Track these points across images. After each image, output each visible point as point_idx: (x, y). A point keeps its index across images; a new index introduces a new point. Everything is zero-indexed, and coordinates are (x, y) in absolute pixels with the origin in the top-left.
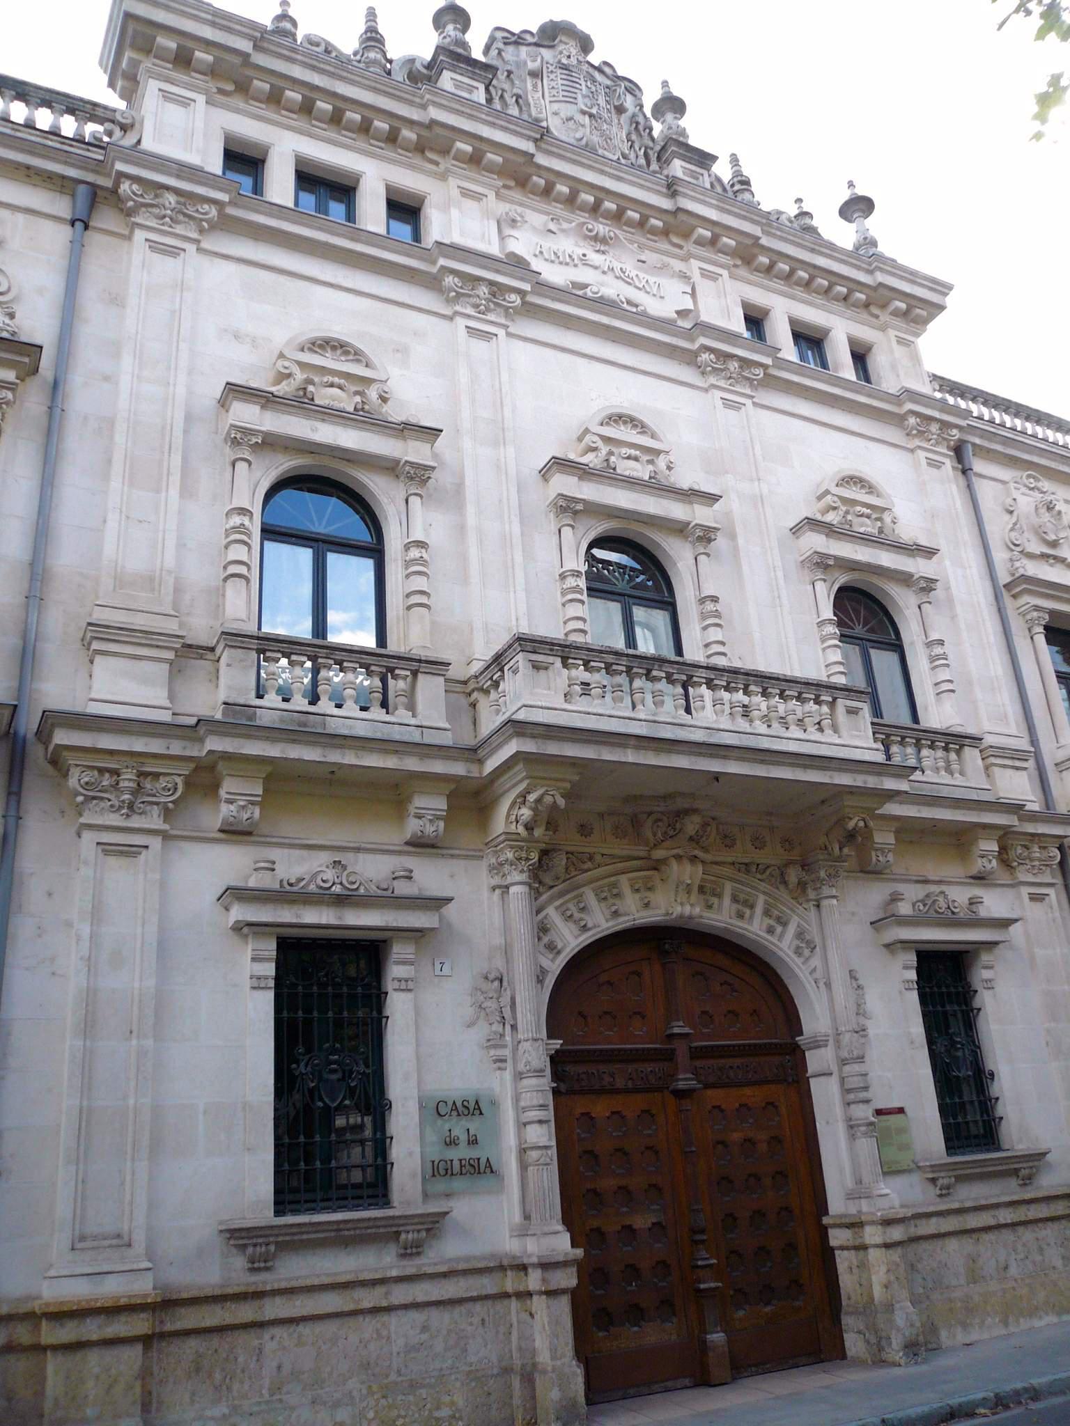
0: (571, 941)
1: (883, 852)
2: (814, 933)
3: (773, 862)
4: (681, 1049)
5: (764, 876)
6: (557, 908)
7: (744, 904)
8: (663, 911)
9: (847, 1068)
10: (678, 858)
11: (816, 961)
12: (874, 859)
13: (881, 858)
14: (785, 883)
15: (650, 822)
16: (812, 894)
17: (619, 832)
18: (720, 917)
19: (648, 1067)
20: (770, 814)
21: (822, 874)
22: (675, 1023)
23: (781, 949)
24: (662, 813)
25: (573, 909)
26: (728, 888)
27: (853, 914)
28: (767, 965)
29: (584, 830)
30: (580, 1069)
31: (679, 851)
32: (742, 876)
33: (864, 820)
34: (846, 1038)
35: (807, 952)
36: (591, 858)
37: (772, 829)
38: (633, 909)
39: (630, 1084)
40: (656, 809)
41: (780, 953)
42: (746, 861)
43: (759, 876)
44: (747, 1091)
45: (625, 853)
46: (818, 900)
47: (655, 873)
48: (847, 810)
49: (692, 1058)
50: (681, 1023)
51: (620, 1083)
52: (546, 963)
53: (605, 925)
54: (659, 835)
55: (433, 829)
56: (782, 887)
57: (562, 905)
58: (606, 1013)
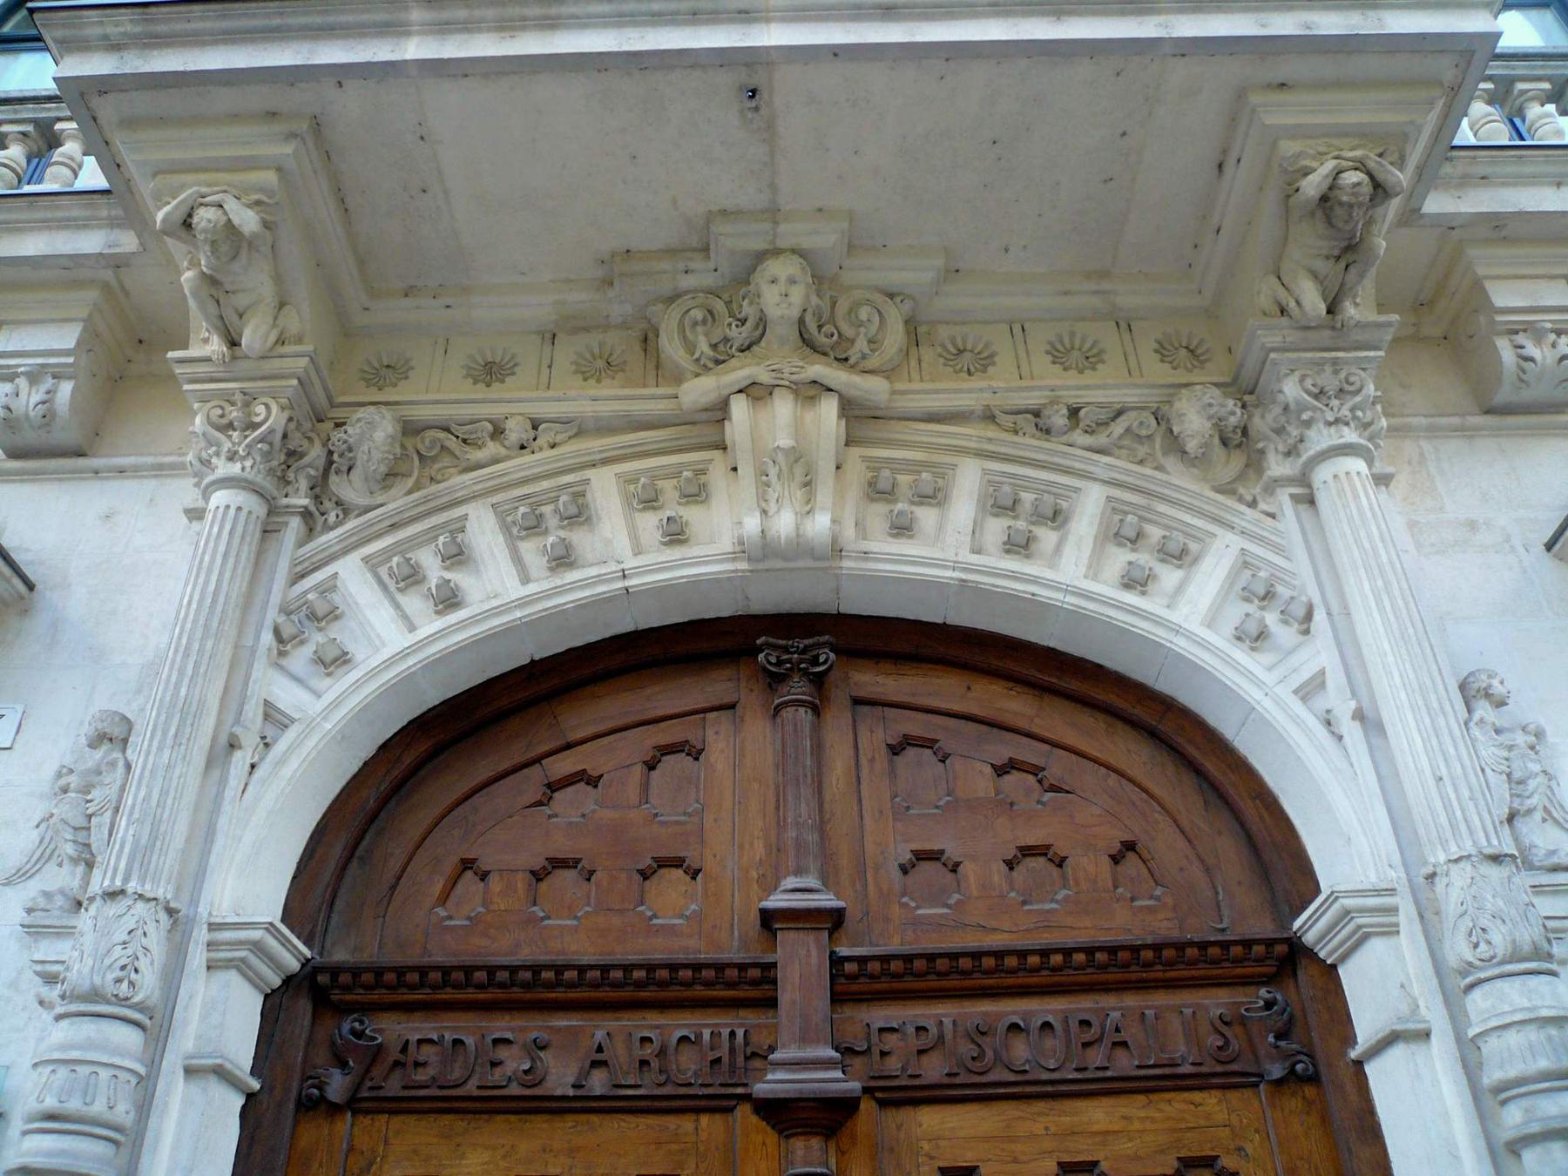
0: (395, 639)
1: (1538, 341)
2: (1302, 576)
3: (1129, 396)
4: (801, 964)
5: (1101, 439)
6: (371, 563)
7: (1028, 518)
8: (726, 544)
9: (1478, 1002)
10: (755, 391)
11: (1319, 654)
12: (1508, 355)
13: (1532, 350)
14: (1175, 445)
15: (675, 313)
16: (1277, 467)
17: (602, 367)
18: (943, 555)
19: (679, 1024)
20: (1104, 274)
21: (1291, 390)
22: (791, 882)
23: (1177, 630)
24: (710, 292)
25: (429, 561)
26: (968, 480)
27: (1472, 526)
28: (1167, 705)
29: (491, 372)
30: (414, 1028)
31: (765, 377)
32: (1030, 444)
33: (1361, 166)
34: (1455, 889)
35: (1284, 634)
36: (498, 432)
37: (1125, 324)
38: (622, 544)
39: (598, 1083)
40: (688, 282)
41: (1180, 644)
42: (1033, 399)
43: (1079, 437)
44: (1098, 1113)
45: (605, 409)
46: (1304, 479)
47: (716, 454)
48: (1289, 147)
49: (838, 999)
50: (811, 881)
51: (560, 1077)
52: (287, 696)
53: (515, 590)
54: (703, 347)
55: (36, 397)
56: (1171, 462)
57: (387, 554)
58: (558, 863)
